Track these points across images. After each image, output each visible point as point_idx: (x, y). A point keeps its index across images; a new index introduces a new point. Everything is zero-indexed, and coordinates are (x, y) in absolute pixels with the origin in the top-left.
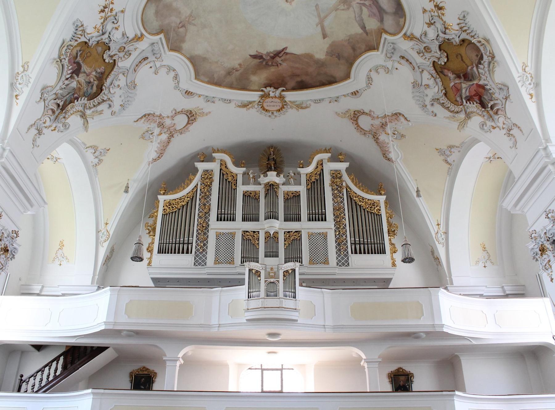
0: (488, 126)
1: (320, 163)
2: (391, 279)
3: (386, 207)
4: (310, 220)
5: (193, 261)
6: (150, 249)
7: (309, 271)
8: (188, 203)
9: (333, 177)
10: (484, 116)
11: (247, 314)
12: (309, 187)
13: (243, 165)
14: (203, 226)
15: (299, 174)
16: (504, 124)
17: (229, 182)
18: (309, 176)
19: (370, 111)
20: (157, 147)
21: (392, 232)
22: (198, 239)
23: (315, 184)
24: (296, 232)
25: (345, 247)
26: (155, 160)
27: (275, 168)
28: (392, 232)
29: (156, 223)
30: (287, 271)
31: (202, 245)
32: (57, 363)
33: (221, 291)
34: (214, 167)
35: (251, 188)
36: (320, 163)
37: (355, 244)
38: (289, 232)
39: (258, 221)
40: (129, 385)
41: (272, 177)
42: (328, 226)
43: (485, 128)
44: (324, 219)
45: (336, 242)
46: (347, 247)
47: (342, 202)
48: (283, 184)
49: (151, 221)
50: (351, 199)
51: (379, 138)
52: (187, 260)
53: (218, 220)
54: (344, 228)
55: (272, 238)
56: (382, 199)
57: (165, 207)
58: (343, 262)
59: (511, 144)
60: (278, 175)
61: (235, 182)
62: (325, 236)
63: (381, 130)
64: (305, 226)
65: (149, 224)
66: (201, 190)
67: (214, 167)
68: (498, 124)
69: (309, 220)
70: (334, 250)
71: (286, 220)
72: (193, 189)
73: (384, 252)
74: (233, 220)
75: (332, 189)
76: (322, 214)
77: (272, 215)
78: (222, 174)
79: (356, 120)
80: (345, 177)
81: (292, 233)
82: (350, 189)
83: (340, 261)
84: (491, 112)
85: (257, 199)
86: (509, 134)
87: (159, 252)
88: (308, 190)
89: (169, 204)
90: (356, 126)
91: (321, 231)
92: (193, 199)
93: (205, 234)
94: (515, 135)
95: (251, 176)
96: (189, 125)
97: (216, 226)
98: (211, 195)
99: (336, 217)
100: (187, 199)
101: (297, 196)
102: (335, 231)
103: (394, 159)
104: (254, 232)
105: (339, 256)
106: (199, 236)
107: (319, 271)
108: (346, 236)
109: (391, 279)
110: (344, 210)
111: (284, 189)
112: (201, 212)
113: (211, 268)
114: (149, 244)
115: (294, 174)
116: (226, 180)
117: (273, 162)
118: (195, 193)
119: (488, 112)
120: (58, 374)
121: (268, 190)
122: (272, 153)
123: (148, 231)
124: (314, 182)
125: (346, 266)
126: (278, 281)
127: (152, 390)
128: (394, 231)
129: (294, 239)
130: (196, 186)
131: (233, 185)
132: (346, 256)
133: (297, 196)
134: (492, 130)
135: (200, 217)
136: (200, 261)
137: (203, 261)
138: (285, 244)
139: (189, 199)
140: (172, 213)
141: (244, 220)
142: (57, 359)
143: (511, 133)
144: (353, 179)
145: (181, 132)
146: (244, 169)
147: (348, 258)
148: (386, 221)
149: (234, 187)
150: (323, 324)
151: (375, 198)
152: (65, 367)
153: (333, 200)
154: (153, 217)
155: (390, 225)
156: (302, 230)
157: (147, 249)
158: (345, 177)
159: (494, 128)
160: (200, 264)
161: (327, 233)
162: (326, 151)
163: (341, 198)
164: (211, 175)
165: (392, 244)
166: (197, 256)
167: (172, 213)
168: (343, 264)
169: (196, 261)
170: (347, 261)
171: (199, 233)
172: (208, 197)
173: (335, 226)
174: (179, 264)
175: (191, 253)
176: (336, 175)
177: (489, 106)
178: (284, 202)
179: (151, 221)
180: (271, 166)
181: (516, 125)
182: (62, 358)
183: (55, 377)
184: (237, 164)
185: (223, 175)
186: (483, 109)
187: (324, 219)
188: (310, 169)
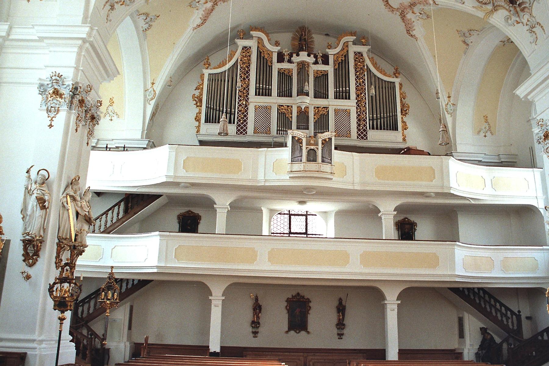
0: (512, 20)
1: (346, 45)
4: (337, 98)
6: (198, 118)
10: (510, 11)
12: (337, 67)
16: (528, 21)
21: (404, 112)
28: (404, 112)
32: (119, 208)
34: (252, 43)
36: (346, 45)
37: (373, 120)
38: (318, 107)
40: (177, 226)
42: (351, 104)
43: (510, 22)
49: (197, 93)
53: (256, 95)
58: (362, 135)
59: (531, 39)
60: (309, 55)
64: (332, 103)
67: (252, 43)
68: (523, 20)
69: (336, 98)
76: (346, 93)
78: (259, 53)
81: (320, 109)
84: (518, 9)
85: (290, 77)
86: (531, 30)
87: (206, 121)
88: (335, 70)
91: (346, 108)
94: (536, 32)
97: (255, 101)
98: (249, 70)
104: (288, 106)
111: (313, 68)
114: (197, 114)
119: (515, 8)
120: (120, 217)
123: (195, 102)
127: (197, 233)
128: (406, 110)
133: (325, 75)
134: (515, 24)
136: (242, 129)
142: (118, 204)
143: (534, 30)
147: (366, 133)
152: (126, 211)
156: (330, 107)
157: (195, 119)
159: (518, 23)
162: (352, 34)
165: (403, 122)
166: (239, 125)
172: (247, 72)
175: (234, 123)
177: (518, 3)
179: (197, 93)
181: (540, 24)
182: (122, 204)
183: (118, 220)
186: (511, 5)
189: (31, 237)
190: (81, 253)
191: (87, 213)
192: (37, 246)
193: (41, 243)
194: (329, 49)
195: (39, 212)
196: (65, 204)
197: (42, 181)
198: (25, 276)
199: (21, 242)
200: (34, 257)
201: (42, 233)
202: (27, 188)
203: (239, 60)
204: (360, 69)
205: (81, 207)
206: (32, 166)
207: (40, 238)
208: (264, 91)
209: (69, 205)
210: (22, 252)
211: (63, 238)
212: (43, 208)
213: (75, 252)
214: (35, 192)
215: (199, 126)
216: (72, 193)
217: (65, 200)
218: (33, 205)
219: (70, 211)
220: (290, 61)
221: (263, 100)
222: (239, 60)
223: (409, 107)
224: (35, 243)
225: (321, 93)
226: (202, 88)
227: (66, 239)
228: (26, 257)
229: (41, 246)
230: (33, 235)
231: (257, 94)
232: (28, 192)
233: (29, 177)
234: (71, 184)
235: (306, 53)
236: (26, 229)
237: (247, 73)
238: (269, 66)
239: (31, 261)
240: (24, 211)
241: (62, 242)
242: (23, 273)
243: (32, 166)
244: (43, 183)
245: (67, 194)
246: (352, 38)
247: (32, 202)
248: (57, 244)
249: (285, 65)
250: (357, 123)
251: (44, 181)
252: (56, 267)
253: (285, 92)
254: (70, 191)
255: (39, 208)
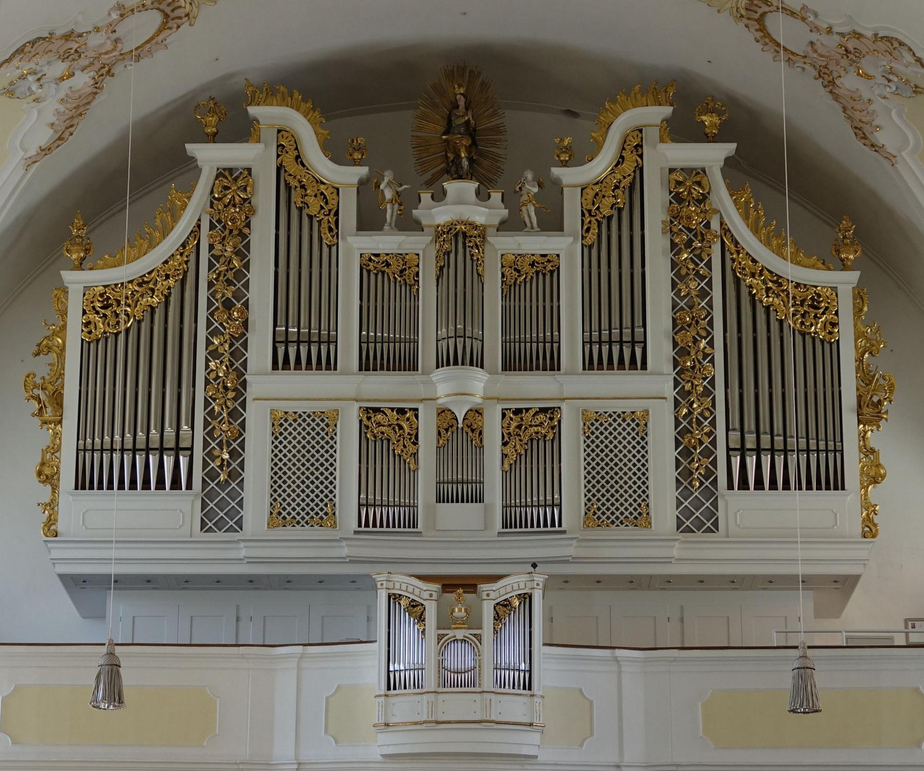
1: (634, 145)
2: (856, 578)
3: (858, 311)
4: (591, 367)
5: (198, 515)
6: (47, 471)
7: (582, 553)
8: (167, 298)
9: (678, 198)
11: (383, 738)
12: (592, 237)
13: (357, 156)
14: (226, 388)
15: (558, 187)
17: (311, 217)
18: (593, 192)
19: (804, 8)
20: (58, 112)
22: (210, 434)
23: (614, 221)
24: (543, 410)
25: (706, 462)
26: (46, 151)
27: (471, 160)
28: (870, 412)
29: (62, 375)
30: (506, 604)
31: (226, 456)
33: (302, 656)
35: (386, 243)
36: (634, 145)
38: (517, 412)
39: (415, 368)
41: (461, 203)
44: (639, 363)
45: (678, 443)
46: (714, 463)
47: (703, 294)
48: (504, 226)
49: (42, 367)
50: (737, 281)
51: (837, 82)
52: (178, 510)
54: (707, 392)
55: (460, 432)
56: (845, 281)
57: (92, 317)
58: (699, 517)
60: (482, 196)
61: (332, 219)
62: (638, 425)
63: (844, 62)
64: (576, 390)
65: (39, 381)
66: (211, 247)
69: (589, 365)
70: (671, 474)
71: (509, 365)
72: (184, 245)
73: (838, 484)
74: (328, 368)
75: (673, 245)
76: (633, 343)
77: (461, 355)
79: (761, 20)
80: (721, 196)
82: (737, 243)
83: (688, 513)
87: (83, 483)
88: (587, 248)
89: (104, 302)
90: (759, 34)
92: (184, 280)
93: (234, 414)
95: (389, 194)
96: (167, 32)
98: (247, 266)
99: (681, 351)
100: (162, 285)
101: (546, 269)
102: (677, 404)
103: (890, 149)
104: (401, 411)
105: (686, 493)
106: (215, 423)
107: (619, 550)
108: (713, 423)
109: (856, 578)
110: (711, 323)
112: (214, 333)
113: (259, 540)
114: (44, 452)
115: (540, 185)
116: (300, 209)
117: (466, 142)
118: (193, 258)
121: (448, 253)
122: (462, 102)
124: (609, 219)
125: (709, 530)
126: (479, 637)
128: (880, 402)
129: (533, 432)
130: (196, 232)
131: (325, 225)
132: (710, 493)
133: (546, 269)
135: (214, 354)
136: (221, 514)
137: (232, 513)
138: (504, 456)
139: (171, 281)
140: (117, 335)
141: (366, 365)
144: (747, 203)
145: (138, 54)
146: (363, 171)
147: (715, 504)
148: (853, 365)
149: (327, 238)
150: (615, 759)
151: (819, 277)
153: (674, 285)
154: (49, 349)
155: (865, 377)
156: (564, 406)
157: (40, 474)
158: (721, 196)
160: (220, 525)
161: (647, 412)
163: (702, 278)
164: (245, 189)
165: (868, 451)
166: (209, 495)
167: (117, 335)
168: (699, 525)
169: (207, 515)
170: (712, 514)
171: (211, 413)
172: (239, 275)
173: (676, 384)
174: (152, 524)
175: (189, 486)
176: (687, 189)
178: (504, 297)
179: (42, 367)
180: (458, 156)
184: (337, 153)
185: (289, 188)
187: (639, 363)
188: (600, 166)
194: (565, 164)
203: (205, 226)
204: (689, 237)
208: (302, 350)
215: (51, 505)
220: (407, 224)
221: (303, 389)
222: (205, 226)
223: (891, 387)
225: (532, 353)
226: (63, 348)
231: (280, 363)
235: (470, 187)
237: (237, 277)
238: (330, 247)
246: (660, 113)
249: (386, 243)
250: (678, 464)
253: (387, 354)
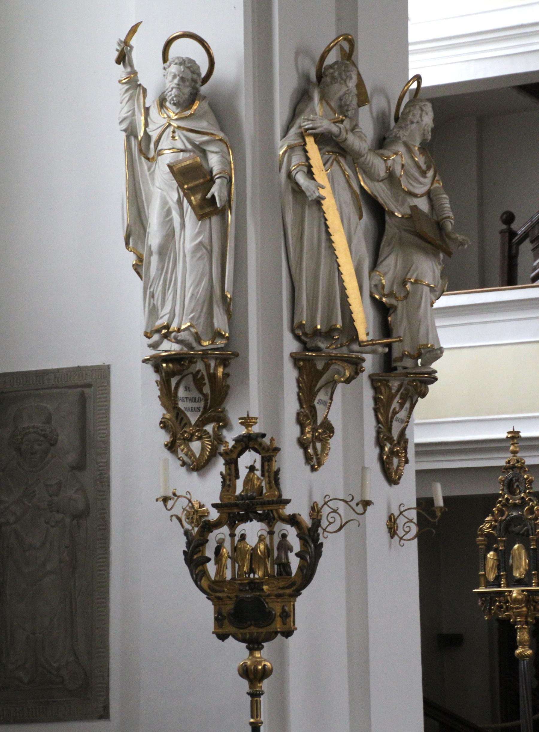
189: (178, 342)
190: (420, 383)
191: (423, 204)
192: (213, 377)
193: (224, 361)
195: (191, 232)
196: (301, 179)
197: (187, 91)
198: (178, 510)
199: (149, 368)
200: (209, 428)
201: (220, 322)
202: (131, 132)
205: (391, 178)
206: (133, 30)
207: (220, 343)
209: (321, 175)
210: (158, 411)
211: (316, 333)
212: (207, 209)
213: (395, 384)
214: (165, 143)
216: (325, 125)
217: (297, 159)
218: (164, 203)
219: (330, 206)
224: (200, 366)
227: (329, 333)
228: (177, 429)
229: (226, 375)
230: (182, 336)
232: (141, 147)
233: (133, 83)
234: (320, 77)
236: (153, 312)
239: (196, 446)
240: (136, 232)
241: (317, 349)
242: (165, 500)
243: (133, 30)
244: (194, 96)
245: (302, 136)
247: (162, 188)
248: (296, 359)
251: (194, 89)
252: (308, 459)
254: (319, 117)
255: (189, 214)
